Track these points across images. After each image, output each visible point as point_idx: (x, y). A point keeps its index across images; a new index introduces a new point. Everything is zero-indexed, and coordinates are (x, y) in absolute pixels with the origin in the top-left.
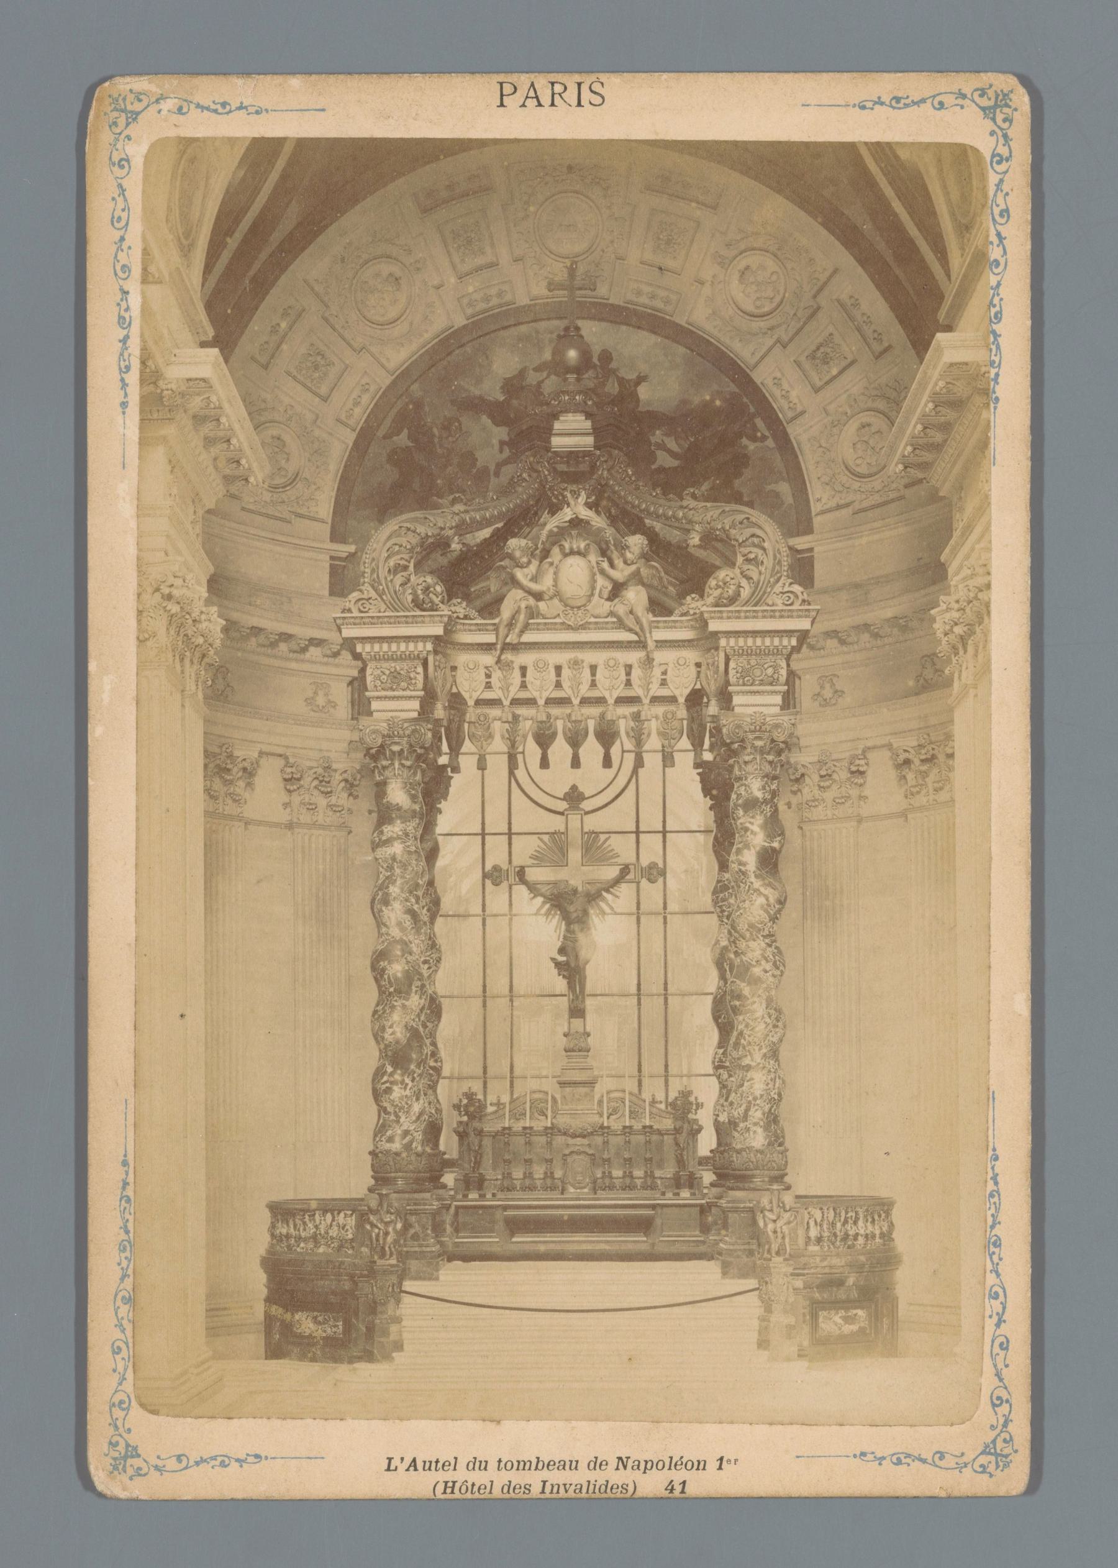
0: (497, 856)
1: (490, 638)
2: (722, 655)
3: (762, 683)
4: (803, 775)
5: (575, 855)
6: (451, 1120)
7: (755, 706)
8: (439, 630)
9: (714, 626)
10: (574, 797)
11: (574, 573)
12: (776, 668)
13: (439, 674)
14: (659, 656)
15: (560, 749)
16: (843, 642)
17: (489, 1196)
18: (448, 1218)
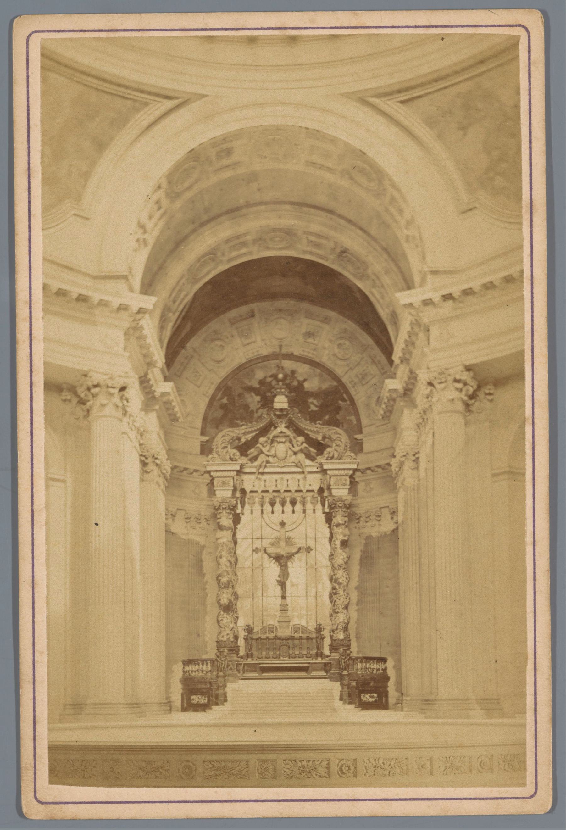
0: (258, 544)
1: (254, 470)
2: (328, 476)
3: (342, 485)
4: (360, 517)
5: (283, 544)
6: (242, 634)
7: (341, 492)
8: (238, 468)
9: (325, 467)
10: (283, 524)
11: (281, 449)
12: (346, 480)
13: (238, 482)
14: (309, 476)
15: (278, 507)
16: (372, 471)
17: (255, 660)
18: (241, 668)
